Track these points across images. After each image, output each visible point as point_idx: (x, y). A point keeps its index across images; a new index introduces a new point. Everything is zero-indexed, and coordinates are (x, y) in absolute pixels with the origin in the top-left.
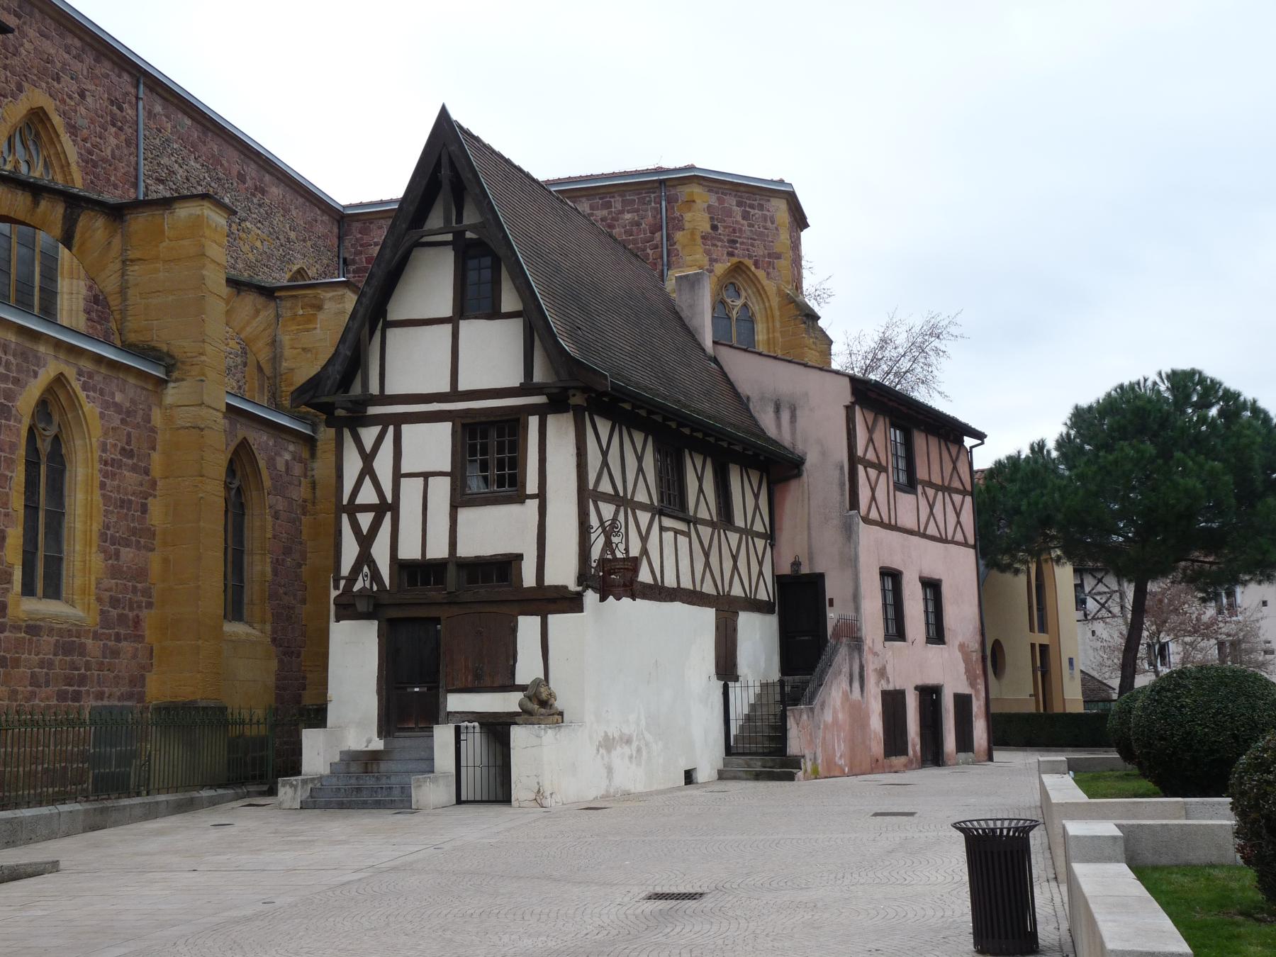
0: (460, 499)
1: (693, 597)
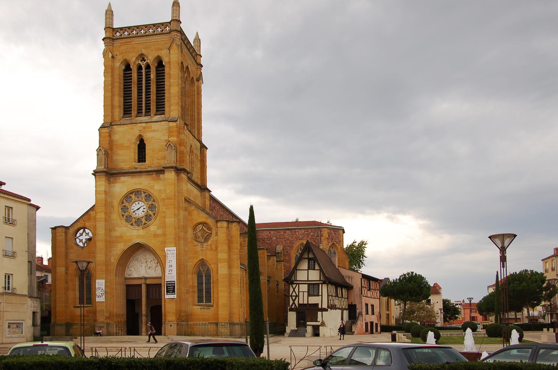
0: (309, 295)
1: (339, 309)
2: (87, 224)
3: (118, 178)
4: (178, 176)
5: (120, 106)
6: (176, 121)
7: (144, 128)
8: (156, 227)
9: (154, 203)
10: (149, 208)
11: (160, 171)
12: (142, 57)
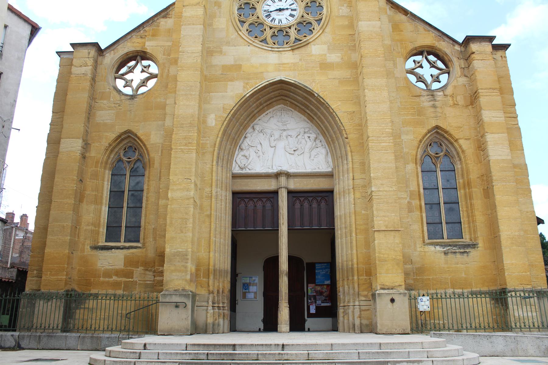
2: (150, 46)
8: (325, 47)
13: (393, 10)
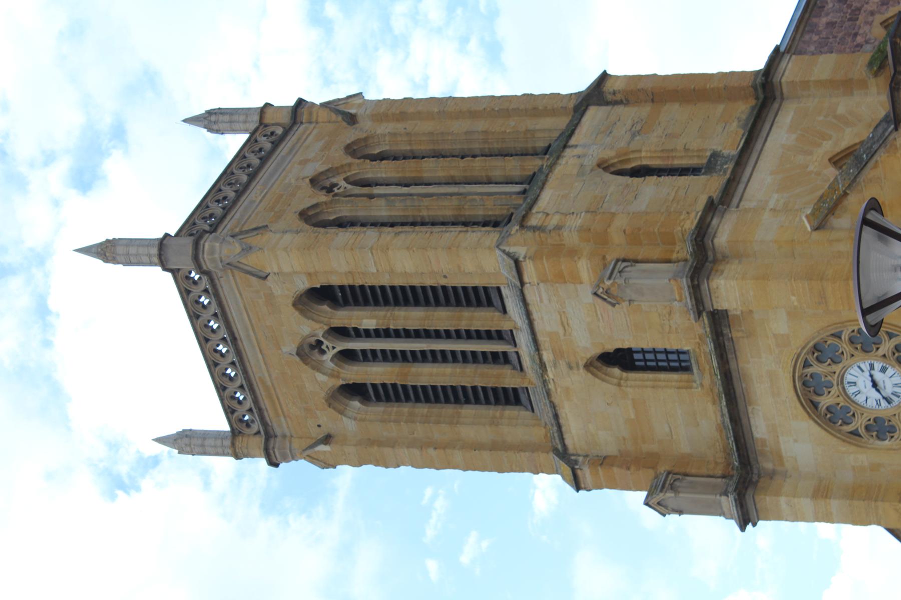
3: (759, 447)
4: (725, 258)
5: (494, 423)
6: (517, 262)
7: (558, 354)
9: (845, 336)
10: (866, 350)
11: (718, 322)
12: (310, 350)
13: (837, 212)
